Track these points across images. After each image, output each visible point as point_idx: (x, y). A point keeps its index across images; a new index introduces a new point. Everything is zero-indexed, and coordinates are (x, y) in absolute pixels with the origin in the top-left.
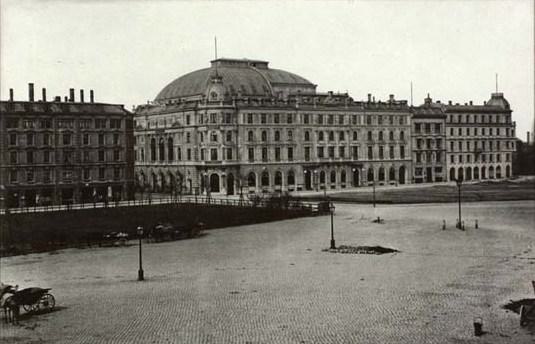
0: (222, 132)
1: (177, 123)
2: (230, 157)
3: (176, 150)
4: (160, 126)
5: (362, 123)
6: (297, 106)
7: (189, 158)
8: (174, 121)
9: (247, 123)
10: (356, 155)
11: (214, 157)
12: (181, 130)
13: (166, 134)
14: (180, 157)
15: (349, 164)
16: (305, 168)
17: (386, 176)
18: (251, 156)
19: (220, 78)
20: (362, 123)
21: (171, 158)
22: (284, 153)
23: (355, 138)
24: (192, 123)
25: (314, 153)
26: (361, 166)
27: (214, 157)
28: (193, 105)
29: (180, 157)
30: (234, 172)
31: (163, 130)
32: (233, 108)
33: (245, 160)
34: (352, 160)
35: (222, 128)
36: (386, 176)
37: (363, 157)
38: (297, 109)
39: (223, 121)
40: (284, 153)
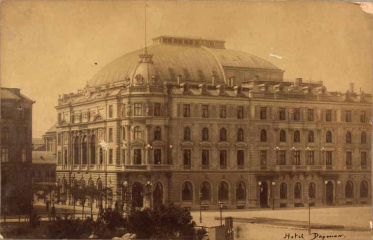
0: (149, 127)
1: (98, 116)
2: (157, 159)
3: (98, 151)
4: (85, 121)
5: (339, 120)
6: (250, 95)
7: (111, 162)
8: (97, 113)
9: (182, 117)
10: (329, 163)
11: (138, 160)
12: (103, 125)
13: (89, 131)
14: (101, 161)
15: (319, 174)
16: (259, 178)
17: (357, 192)
18: (187, 160)
19: (151, 56)
20: (339, 120)
21: (93, 162)
22: (232, 159)
23: (329, 140)
24: (115, 116)
25: (272, 159)
26: (336, 177)
27: (138, 160)
28: (116, 92)
29: (101, 161)
30: (163, 181)
31: (86, 125)
32: (165, 96)
33: (177, 165)
34: (324, 168)
35: (148, 122)
36: (357, 192)
37: (339, 165)
38: (250, 100)
39: (149, 113)
40: (232, 159)
